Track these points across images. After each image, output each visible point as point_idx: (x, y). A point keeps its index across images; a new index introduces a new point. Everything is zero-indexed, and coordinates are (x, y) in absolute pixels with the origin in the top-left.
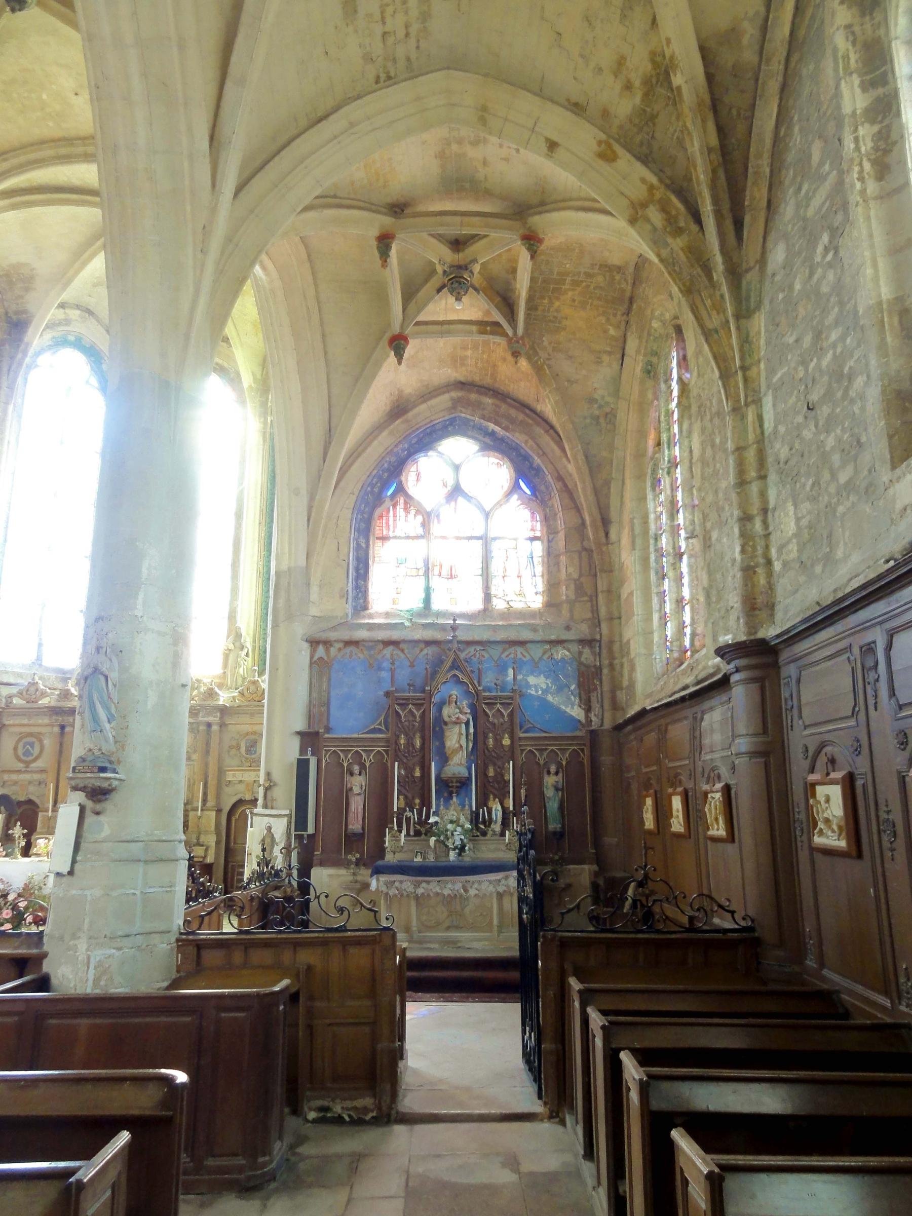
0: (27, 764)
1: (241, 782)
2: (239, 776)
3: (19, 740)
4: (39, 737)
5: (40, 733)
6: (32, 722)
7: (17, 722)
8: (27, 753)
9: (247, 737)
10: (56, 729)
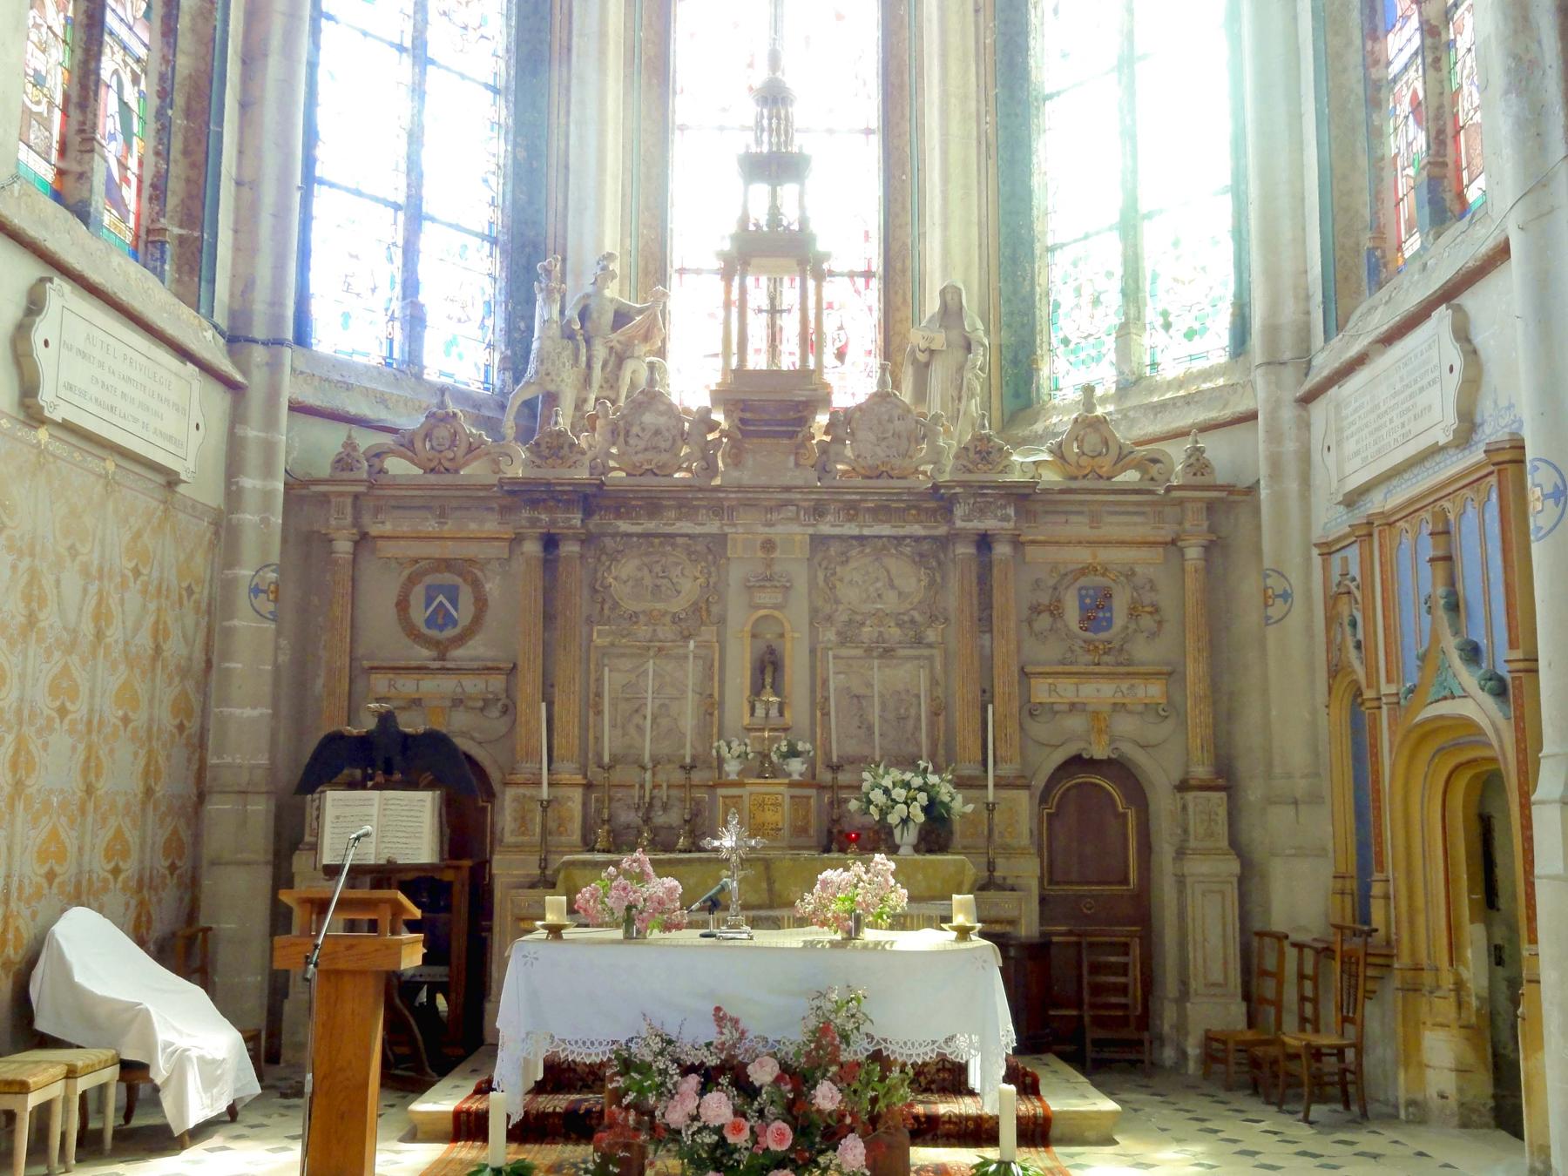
0: (442, 649)
1: (1073, 706)
2: (1067, 690)
3: (412, 581)
4: (463, 568)
5: (471, 561)
6: (449, 528)
7: (405, 528)
8: (441, 619)
9: (1083, 581)
10: (532, 548)
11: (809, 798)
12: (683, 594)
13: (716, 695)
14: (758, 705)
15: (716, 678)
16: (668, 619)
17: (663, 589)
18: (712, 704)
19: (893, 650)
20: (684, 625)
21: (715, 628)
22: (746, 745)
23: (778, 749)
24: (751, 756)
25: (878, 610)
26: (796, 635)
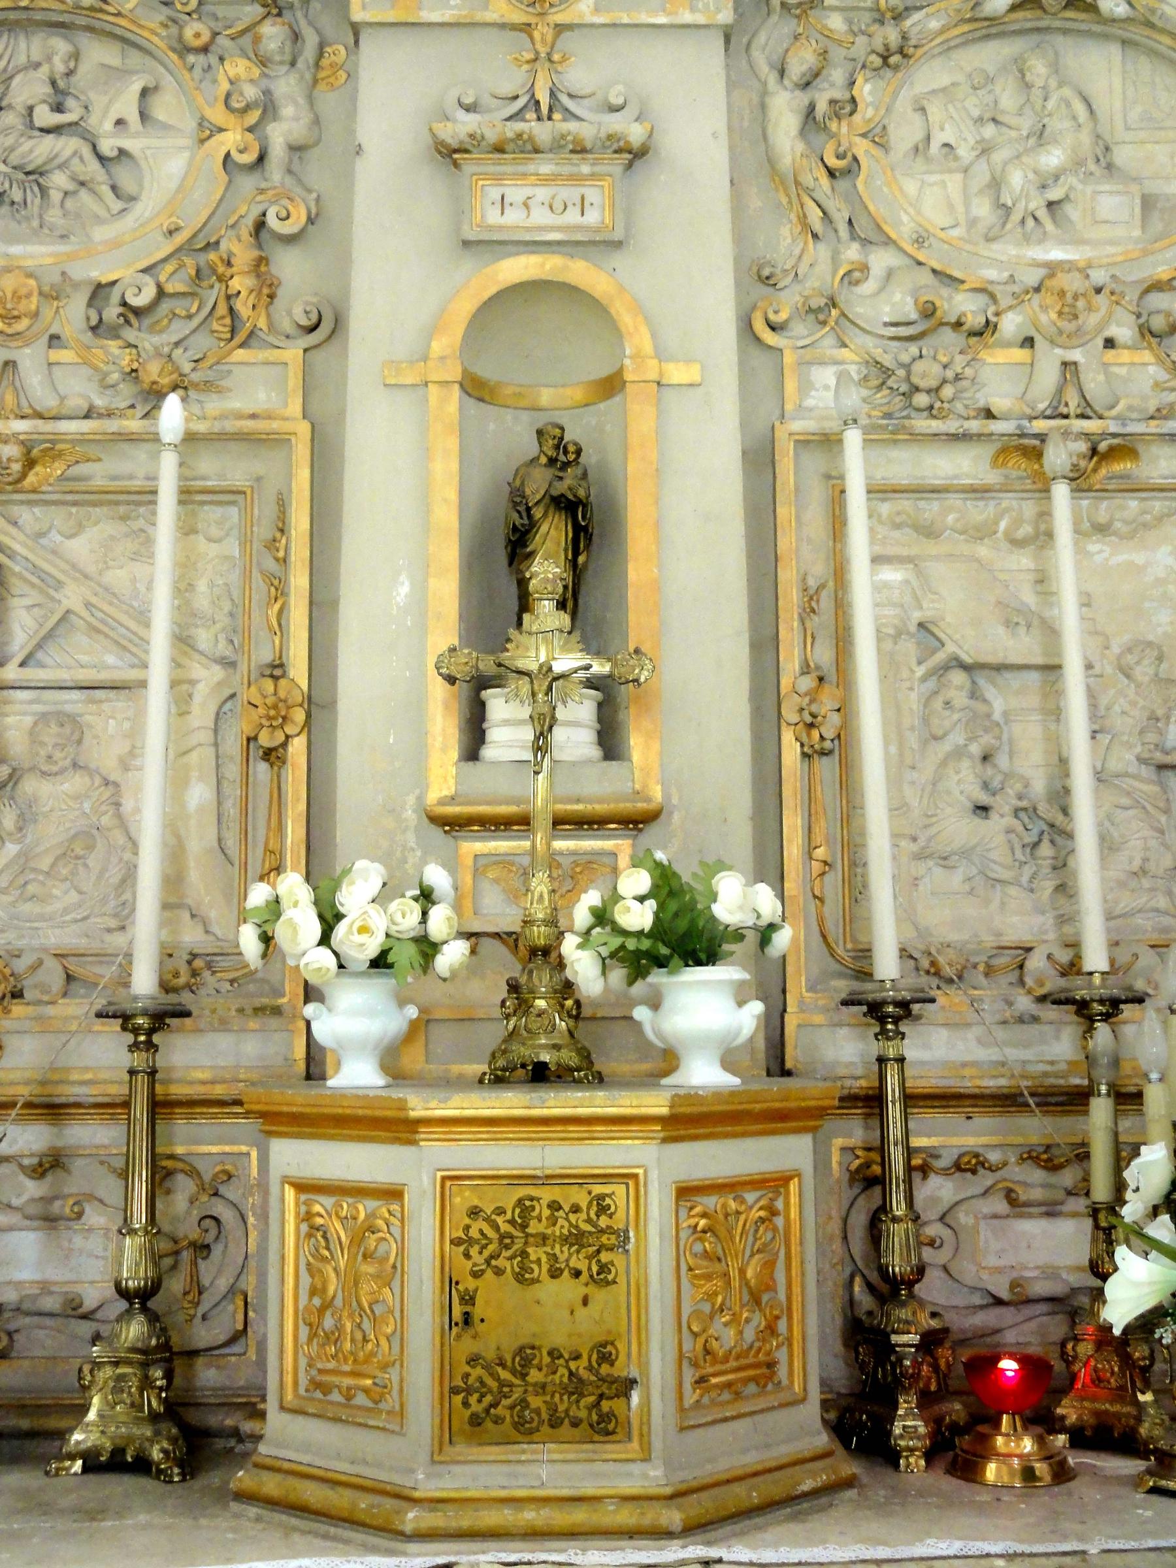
11: (776, 1183)
12: (144, 209)
13: (299, 671)
14: (498, 705)
15: (299, 581)
16: (75, 312)
17: (59, 180)
18: (278, 715)
19: (1124, 449)
20: (148, 342)
21: (293, 354)
22: (426, 897)
23: (601, 917)
24: (453, 954)
25: (1052, 268)
26: (677, 374)
